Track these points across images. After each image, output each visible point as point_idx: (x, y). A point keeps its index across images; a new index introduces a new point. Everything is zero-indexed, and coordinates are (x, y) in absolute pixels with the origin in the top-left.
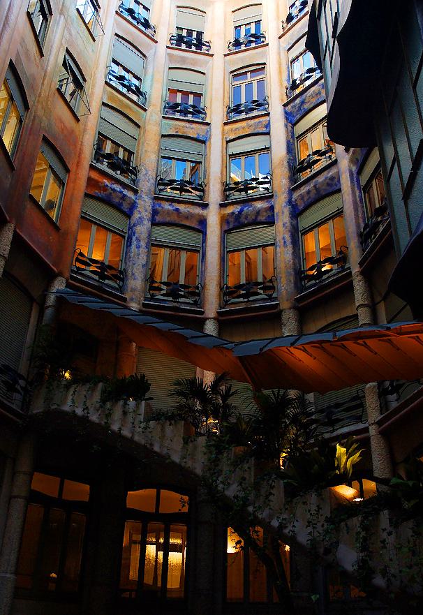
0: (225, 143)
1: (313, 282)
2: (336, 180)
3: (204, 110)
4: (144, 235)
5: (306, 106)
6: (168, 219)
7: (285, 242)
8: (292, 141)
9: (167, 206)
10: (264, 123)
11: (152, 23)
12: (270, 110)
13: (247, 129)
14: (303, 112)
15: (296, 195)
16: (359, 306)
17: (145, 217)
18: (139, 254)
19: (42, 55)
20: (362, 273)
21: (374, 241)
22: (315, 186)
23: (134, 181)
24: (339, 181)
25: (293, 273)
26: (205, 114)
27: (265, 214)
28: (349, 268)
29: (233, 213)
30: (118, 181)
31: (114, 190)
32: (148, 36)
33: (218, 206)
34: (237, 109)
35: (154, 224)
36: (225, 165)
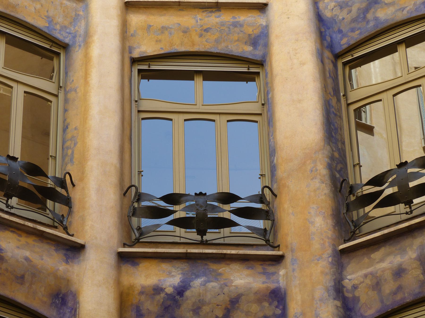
0: (127, 62)
8: (334, 102)
10: (250, 31)
13: (196, 39)
14: (370, 28)
27: (254, 308)
29: (158, 290)
33: (112, 259)
36: (127, 132)
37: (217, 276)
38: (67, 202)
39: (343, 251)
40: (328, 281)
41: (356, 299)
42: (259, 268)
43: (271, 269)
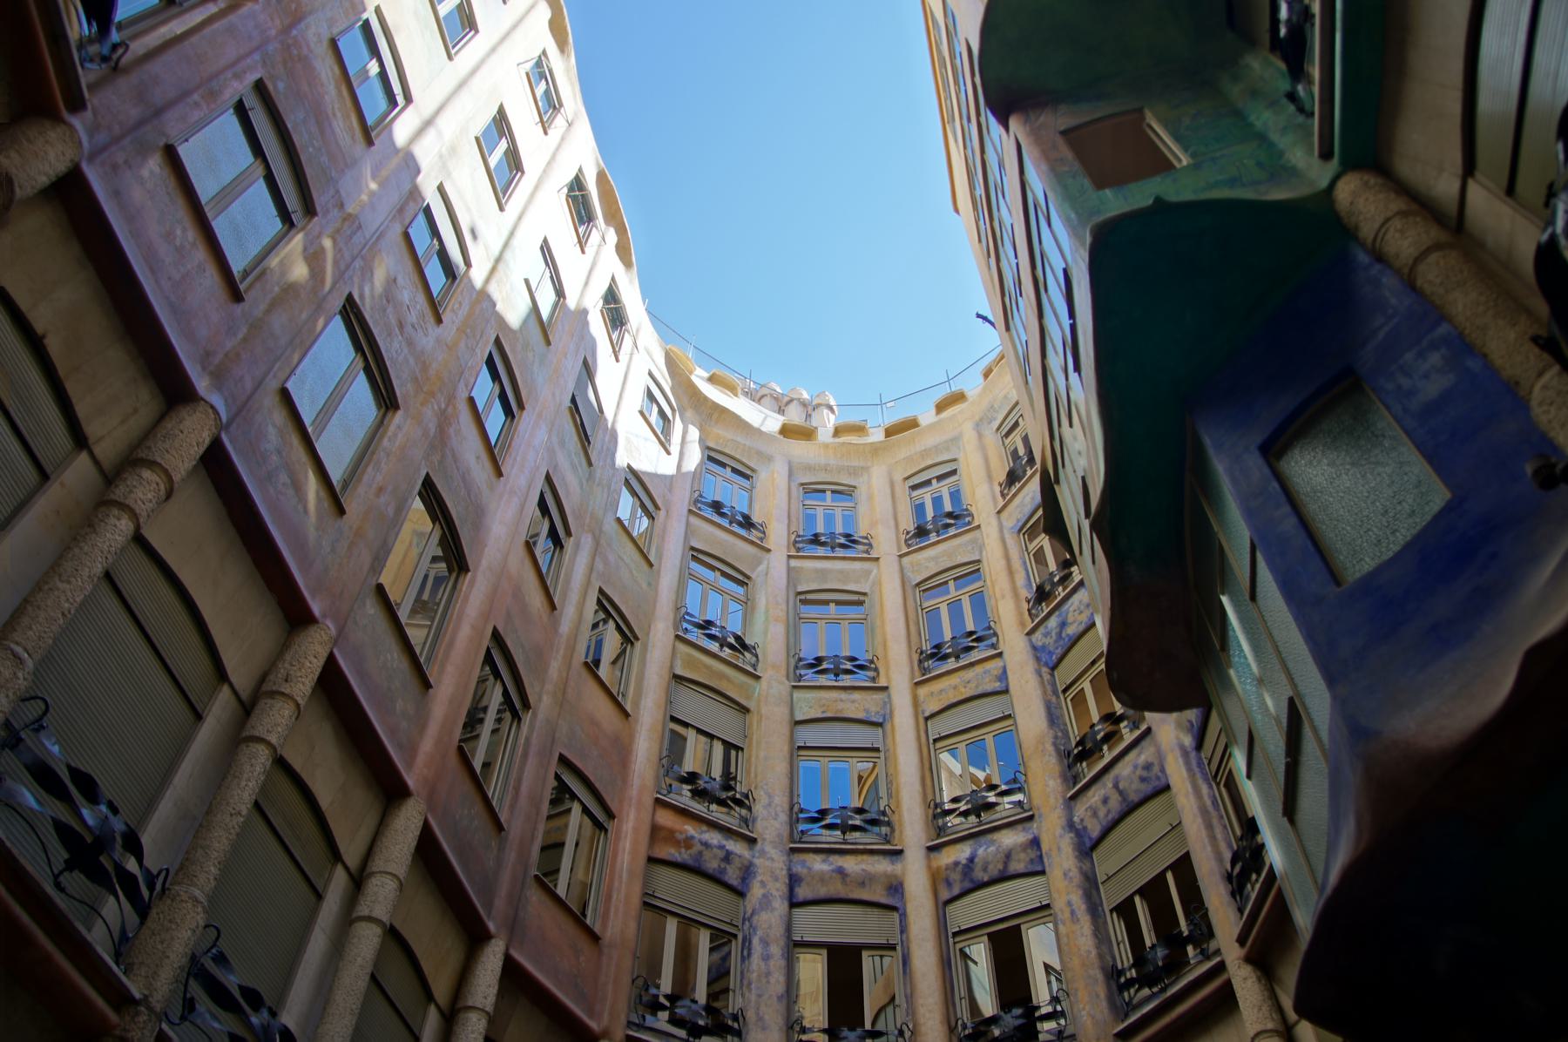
0: (922, 721)
1: (1146, 992)
2: (1156, 769)
3: (872, 662)
4: (778, 931)
5: (1072, 630)
6: (823, 892)
7: (1073, 913)
8: (1054, 699)
9: (819, 864)
11: (755, 519)
12: (1002, 647)
15: (1081, 810)
16: (1257, 1035)
17: (775, 893)
18: (768, 974)
19: (553, 607)
20: (1249, 959)
21: (1258, 886)
22: (1116, 786)
23: (745, 821)
24: (1163, 770)
25: (1100, 976)
26: (876, 670)
27: (1022, 856)
28: (1218, 952)
29: (956, 864)
30: (714, 825)
31: (706, 845)
32: (752, 543)
33: (923, 852)
34: (938, 654)
35: (794, 904)
37: (993, 842)
38: (889, 824)
39: (1073, 798)
40: (1063, 821)
41: (1085, 828)
42: (1020, 827)
43: (1028, 825)
